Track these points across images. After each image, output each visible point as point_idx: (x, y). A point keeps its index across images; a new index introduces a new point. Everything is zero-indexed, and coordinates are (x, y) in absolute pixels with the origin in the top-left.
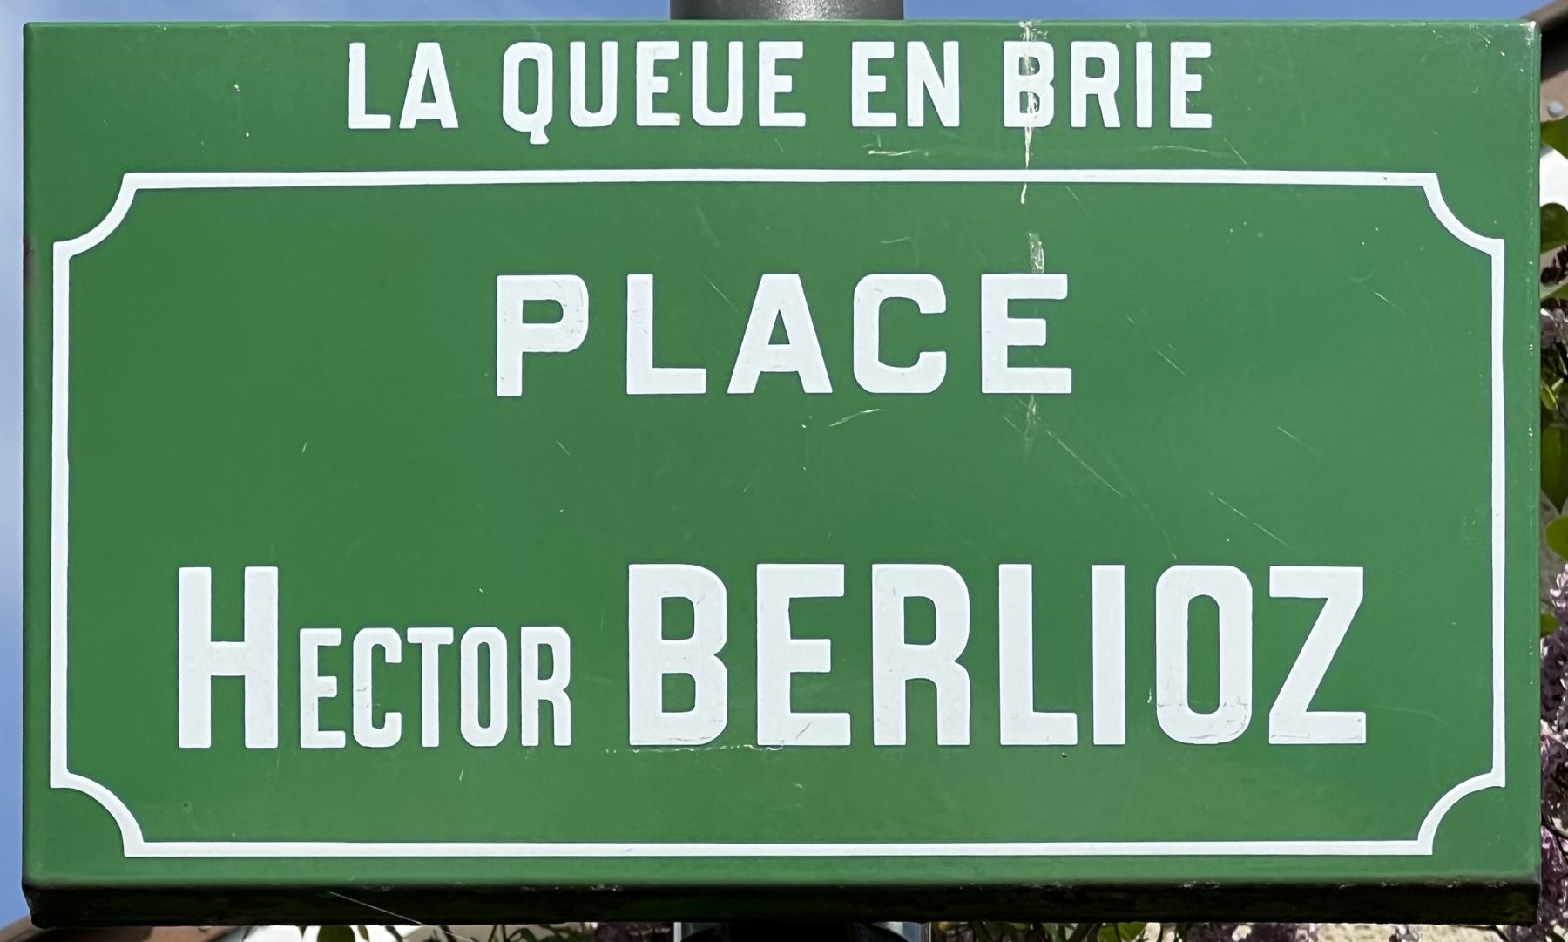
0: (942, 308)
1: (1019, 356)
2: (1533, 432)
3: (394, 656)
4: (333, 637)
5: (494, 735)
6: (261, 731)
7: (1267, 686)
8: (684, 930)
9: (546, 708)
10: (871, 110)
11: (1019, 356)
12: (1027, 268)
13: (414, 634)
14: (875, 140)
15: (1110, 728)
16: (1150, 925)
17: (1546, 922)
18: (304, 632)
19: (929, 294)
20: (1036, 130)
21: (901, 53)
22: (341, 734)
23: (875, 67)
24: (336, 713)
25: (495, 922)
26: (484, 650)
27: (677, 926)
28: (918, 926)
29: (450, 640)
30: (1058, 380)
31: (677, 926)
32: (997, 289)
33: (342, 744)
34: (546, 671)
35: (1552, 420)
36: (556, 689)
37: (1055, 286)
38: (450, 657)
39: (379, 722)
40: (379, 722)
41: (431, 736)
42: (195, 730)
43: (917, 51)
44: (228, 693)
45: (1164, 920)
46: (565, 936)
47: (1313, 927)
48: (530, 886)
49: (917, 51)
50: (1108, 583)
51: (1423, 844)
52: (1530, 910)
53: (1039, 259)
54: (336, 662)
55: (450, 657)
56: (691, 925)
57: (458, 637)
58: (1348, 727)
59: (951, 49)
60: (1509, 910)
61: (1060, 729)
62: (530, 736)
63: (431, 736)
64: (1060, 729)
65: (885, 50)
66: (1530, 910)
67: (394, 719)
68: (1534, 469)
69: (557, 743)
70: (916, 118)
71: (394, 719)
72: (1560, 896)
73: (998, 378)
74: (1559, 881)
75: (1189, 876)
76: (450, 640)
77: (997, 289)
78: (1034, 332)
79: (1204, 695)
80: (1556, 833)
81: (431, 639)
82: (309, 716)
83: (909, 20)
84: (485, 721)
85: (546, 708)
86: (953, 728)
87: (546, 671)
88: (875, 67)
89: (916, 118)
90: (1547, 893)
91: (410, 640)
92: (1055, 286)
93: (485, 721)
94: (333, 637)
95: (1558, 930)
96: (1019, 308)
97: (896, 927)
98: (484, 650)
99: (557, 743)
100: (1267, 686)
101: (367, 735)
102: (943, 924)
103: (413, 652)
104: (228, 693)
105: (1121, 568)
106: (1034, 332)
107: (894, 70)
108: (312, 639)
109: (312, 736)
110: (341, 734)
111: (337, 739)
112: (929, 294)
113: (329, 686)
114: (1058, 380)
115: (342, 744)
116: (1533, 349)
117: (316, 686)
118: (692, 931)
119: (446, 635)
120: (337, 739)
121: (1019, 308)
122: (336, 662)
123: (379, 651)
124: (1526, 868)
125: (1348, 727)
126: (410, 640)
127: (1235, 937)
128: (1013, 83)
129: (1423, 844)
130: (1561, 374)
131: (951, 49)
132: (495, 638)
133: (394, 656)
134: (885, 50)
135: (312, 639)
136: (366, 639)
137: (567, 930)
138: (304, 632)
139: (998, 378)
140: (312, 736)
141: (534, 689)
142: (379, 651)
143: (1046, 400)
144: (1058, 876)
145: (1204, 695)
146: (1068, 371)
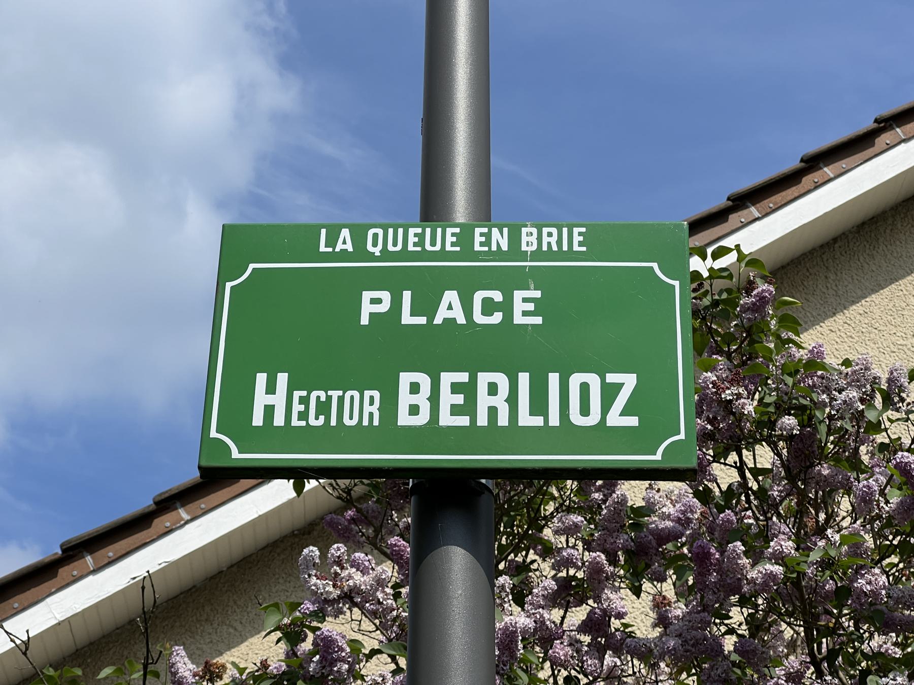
0: (501, 300)
1: (525, 313)
2: (690, 335)
3: (323, 399)
4: (304, 393)
5: (354, 422)
6: (279, 420)
7: (606, 408)
8: (413, 481)
9: (371, 415)
10: (480, 246)
11: (525, 313)
12: (529, 289)
13: (330, 393)
14: (481, 254)
15: (554, 420)
16: (568, 481)
17: (702, 480)
18: (295, 392)
19: (497, 296)
20: (531, 251)
21: (490, 231)
22: (305, 422)
23: (482, 235)
24: (303, 416)
25: (351, 479)
26: (352, 397)
27: (411, 480)
28: (490, 481)
29: (341, 394)
30: (538, 320)
31: (411, 480)
32: (518, 295)
33: (305, 425)
34: (372, 403)
35: (697, 331)
36: (375, 409)
37: (537, 294)
38: (341, 399)
39: (317, 418)
40: (317, 418)
41: (333, 422)
42: (258, 420)
43: (495, 231)
44: (269, 410)
45: (573, 480)
46: (374, 482)
47: (622, 481)
48: (363, 468)
49: (495, 231)
50: (554, 379)
51: (658, 457)
52: (695, 477)
53: (532, 286)
54: (304, 401)
55: (341, 399)
56: (415, 480)
57: (344, 394)
58: (633, 421)
59: (505, 230)
60: (688, 477)
61: (538, 421)
62: (366, 422)
63: (333, 422)
64: (538, 421)
65: (485, 230)
66: (695, 477)
67: (322, 418)
68: (691, 345)
69: (374, 425)
70: (494, 248)
71: (322, 418)
72: (706, 472)
73: (518, 319)
74: (705, 468)
75: (580, 466)
76: (341, 394)
77: (518, 295)
78: (531, 307)
79: (585, 410)
80: (704, 453)
81: (335, 394)
82: (295, 416)
83: (493, 222)
84: (351, 418)
85: (371, 415)
86: (503, 420)
87: (372, 403)
88: (482, 235)
89: (494, 248)
90: (701, 471)
91: (329, 394)
92: (537, 294)
93: (351, 418)
94: (304, 393)
95: (706, 483)
96: (525, 300)
97: (483, 481)
98: (352, 397)
99: (374, 425)
100: (606, 408)
101: (312, 422)
102: (499, 480)
103: (329, 398)
104: (269, 410)
105: (558, 374)
106: (531, 307)
107: (488, 236)
108: (297, 394)
109: (295, 422)
110: (305, 422)
111: (303, 423)
112: (497, 296)
113: (302, 408)
114: (538, 320)
115: (305, 425)
116: (689, 311)
117: (297, 408)
118: (415, 482)
119: (340, 393)
120: (303, 423)
121: (525, 300)
122: (304, 401)
123: (318, 398)
124: (693, 464)
125: (633, 421)
126: (329, 394)
127: (597, 484)
128: (524, 239)
129: (658, 457)
130: (700, 318)
131: (505, 230)
132: (356, 394)
133: (323, 399)
134: (485, 230)
135: (297, 394)
136: (314, 394)
137: (375, 481)
138: (295, 392)
139: (518, 319)
140: (295, 422)
141: (367, 409)
142: (318, 398)
143: (534, 326)
144: (537, 466)
145: (585, 410)
146: (541, 318)
